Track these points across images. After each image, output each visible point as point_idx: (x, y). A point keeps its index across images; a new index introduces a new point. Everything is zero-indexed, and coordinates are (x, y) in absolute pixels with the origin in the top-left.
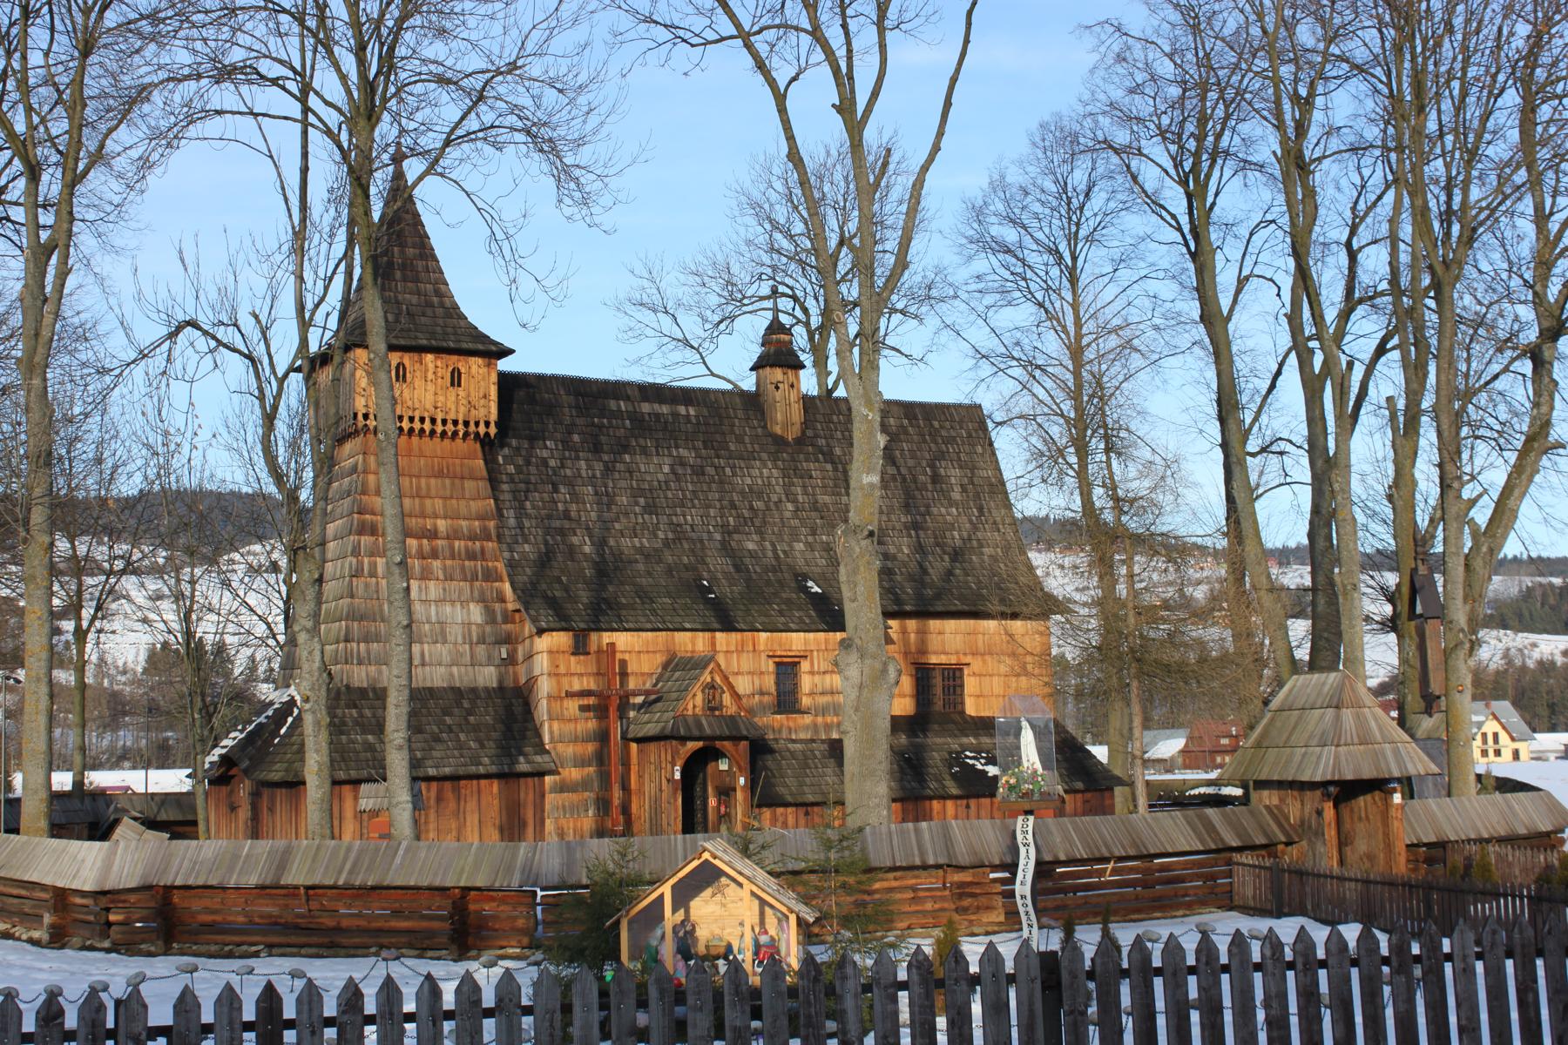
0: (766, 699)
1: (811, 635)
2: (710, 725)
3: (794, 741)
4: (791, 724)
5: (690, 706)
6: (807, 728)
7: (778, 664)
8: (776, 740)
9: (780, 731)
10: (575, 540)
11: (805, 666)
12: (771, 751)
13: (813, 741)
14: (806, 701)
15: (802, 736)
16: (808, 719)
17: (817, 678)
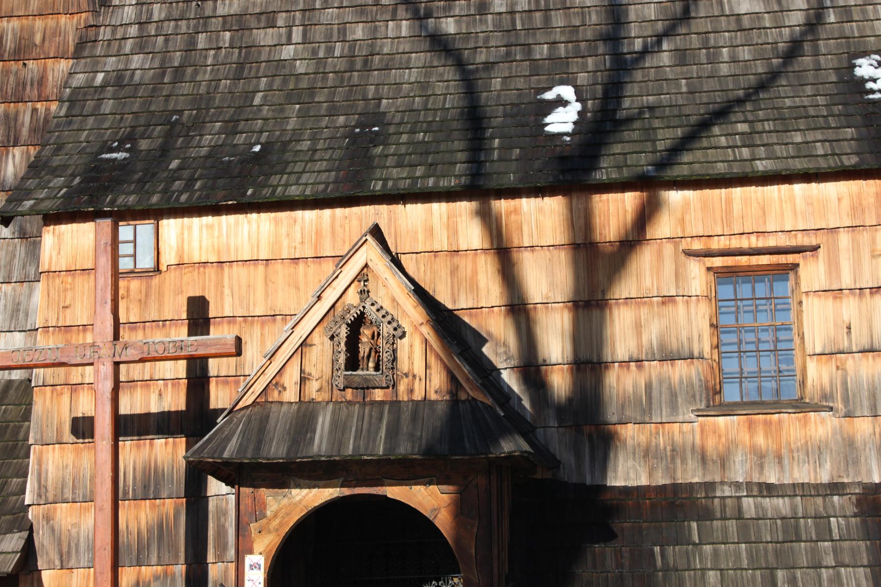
0: (680, 371)
1: (831, 189)
2: (338, 427)
3: (768, 490)
4: (760, 440)
5: (291, 377)
6: (815, 452)
7: (723, 275)
8: (710, 486)
9: (724, 461)
10: (265, 37)
11: (812, 273)
12: (705, 515)
13: (835, 488)
14: (818, 375)
15: (802, 474)
16: (822, 426)
17: (850, 308)
